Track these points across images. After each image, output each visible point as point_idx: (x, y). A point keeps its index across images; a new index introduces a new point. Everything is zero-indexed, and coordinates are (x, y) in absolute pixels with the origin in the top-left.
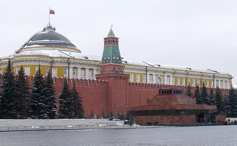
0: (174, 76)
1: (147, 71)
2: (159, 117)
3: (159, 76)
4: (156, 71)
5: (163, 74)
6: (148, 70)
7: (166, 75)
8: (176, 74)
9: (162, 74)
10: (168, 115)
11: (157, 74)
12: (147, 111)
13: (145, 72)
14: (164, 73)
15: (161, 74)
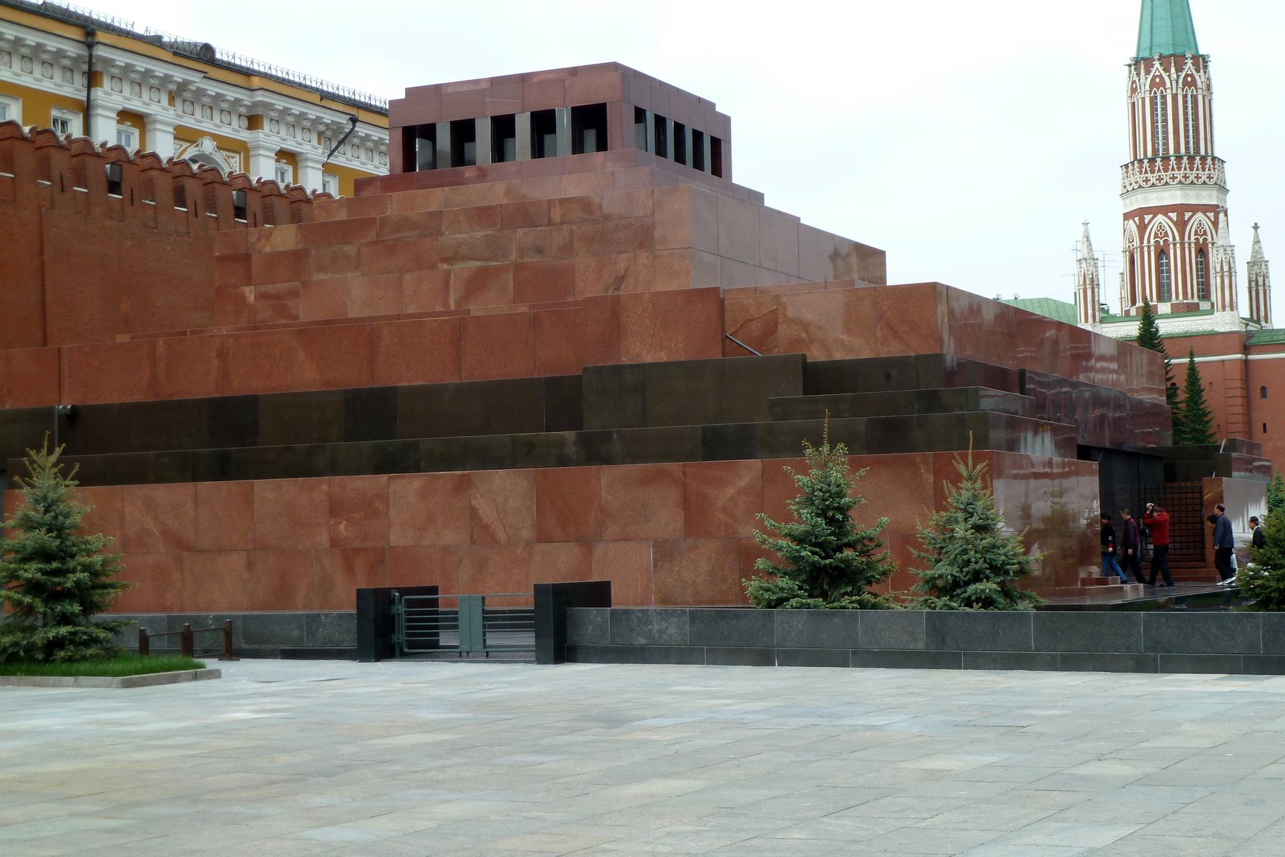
0: (339, 160)
1: (92, 79)
2: (504, 493)
3: (208, 146)
4: (183, 86)
5: (244, 135)
6: (109, 62)
7: (270, 138)
8: (346, 148)
9: (235, 130)
10: (687, 456)
11: (188, 122)
12: (251, 401)
13: (80, 81)
14: (253, 122)
15: (226, 131)
